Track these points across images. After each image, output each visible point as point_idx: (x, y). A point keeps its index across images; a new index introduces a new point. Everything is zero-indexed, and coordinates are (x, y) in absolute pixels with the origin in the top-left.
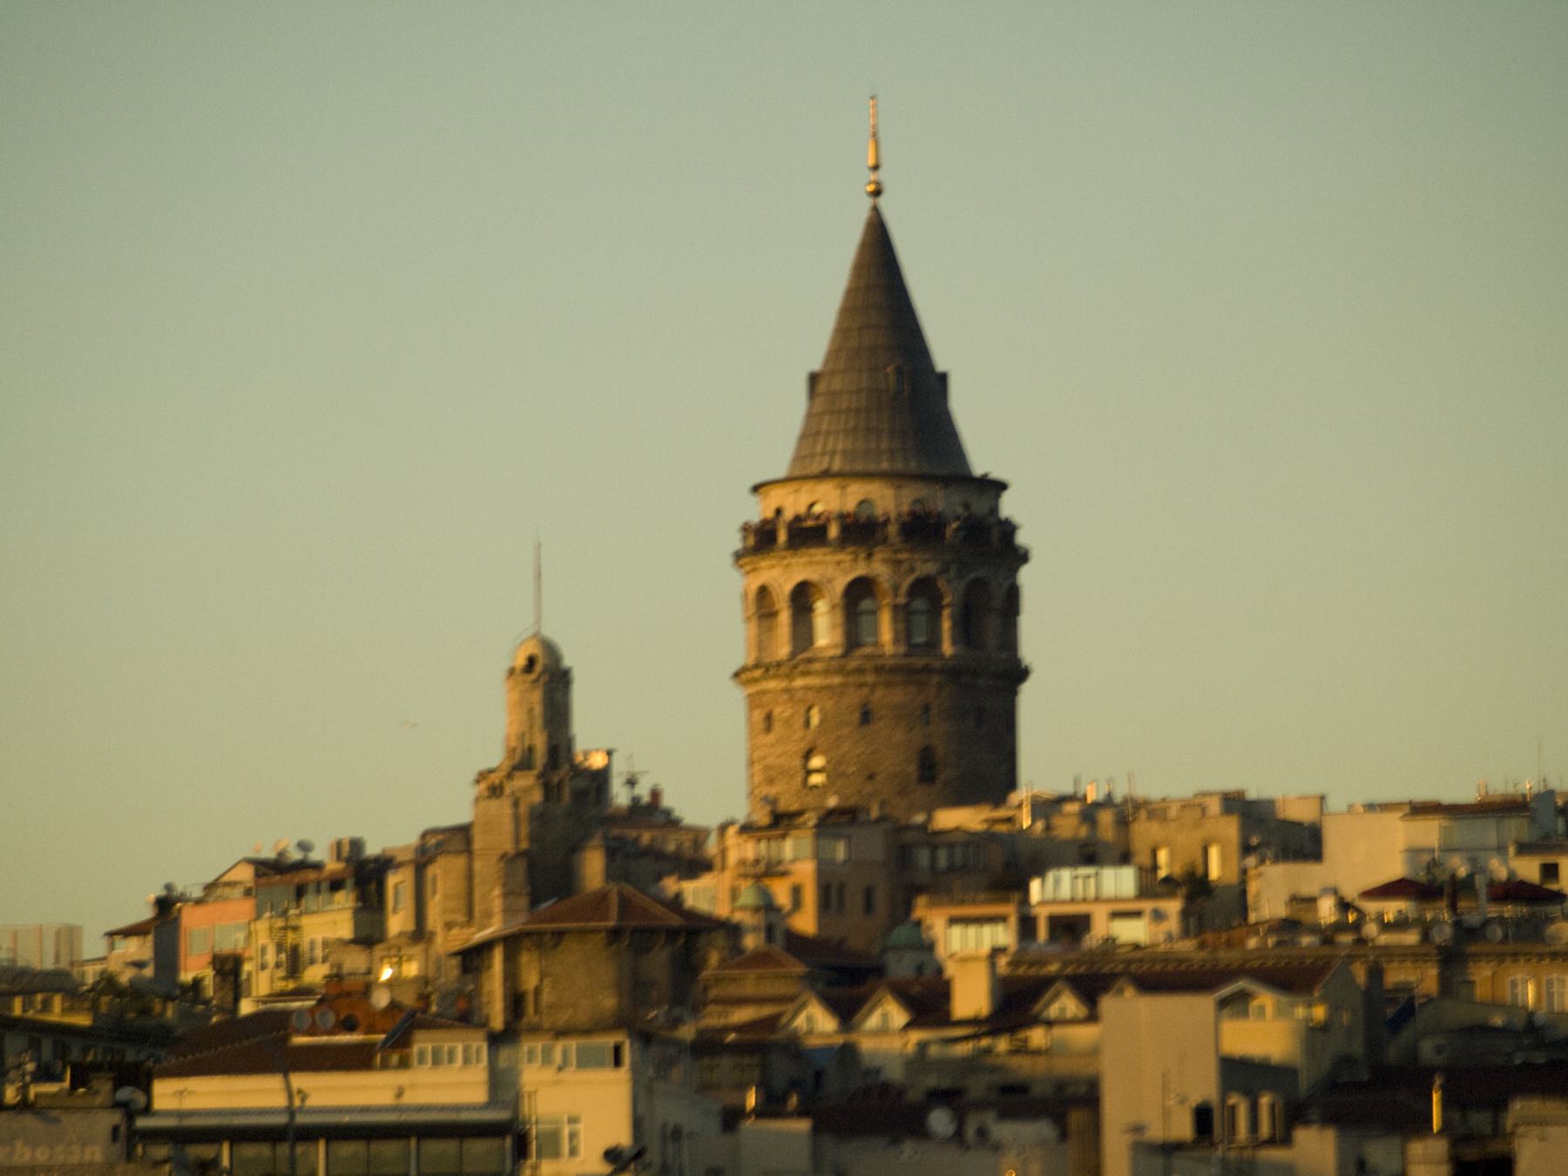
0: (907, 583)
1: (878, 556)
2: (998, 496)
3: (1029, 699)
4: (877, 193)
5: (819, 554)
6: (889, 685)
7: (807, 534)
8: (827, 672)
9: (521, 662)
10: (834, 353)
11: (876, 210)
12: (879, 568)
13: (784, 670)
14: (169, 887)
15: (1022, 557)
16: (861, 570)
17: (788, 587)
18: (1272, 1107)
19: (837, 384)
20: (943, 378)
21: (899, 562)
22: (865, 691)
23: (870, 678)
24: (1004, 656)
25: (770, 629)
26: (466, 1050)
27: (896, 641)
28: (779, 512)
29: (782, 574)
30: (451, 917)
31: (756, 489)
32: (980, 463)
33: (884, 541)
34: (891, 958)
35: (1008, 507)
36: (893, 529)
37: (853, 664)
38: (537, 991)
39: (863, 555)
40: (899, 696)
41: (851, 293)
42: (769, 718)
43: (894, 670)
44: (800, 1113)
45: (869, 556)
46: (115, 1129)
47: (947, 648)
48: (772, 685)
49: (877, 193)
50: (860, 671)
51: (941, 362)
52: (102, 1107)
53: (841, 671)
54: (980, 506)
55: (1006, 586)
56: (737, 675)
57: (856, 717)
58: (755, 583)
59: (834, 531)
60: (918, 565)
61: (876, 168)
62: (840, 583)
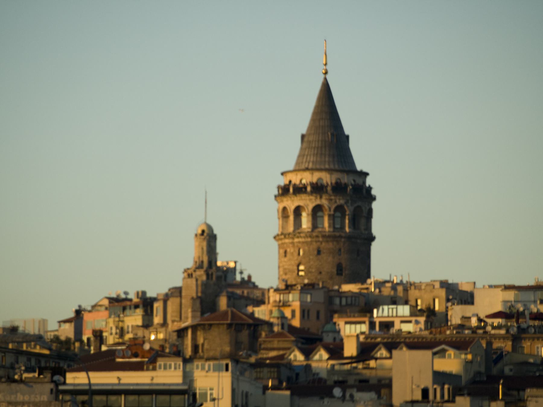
0: (334, 207)
1: (324, 197)
2: (366, 177)
3: (374, 247)
4: (326, 73)
5: (304, 196)
6: (327, 241)
7: (299, 190)
8: (306, 237)
9: (200, 232)
10: (310, 128)
11: (326, 79)
12: (324, 202)
13: (291, 236)
14: (80, 306)
15: (374, 198)
16: (318, 202)
17: (293, 208)
18: (449, 389)
19: (311, 138)
20: (347, 137)
21: (331, 200)
22: (319, 244)
23: (321, 239)
24: (366, 232)
25: (287, 222)
26: (175, 364)
27: (329, 226)
28: (290, 182)
29: (291, 203)
30: (174, 319)
31: (282, 174)
32: (360, 166)
33: (327, 192)
34: (324, 335)
35: (369, 181)
36: (329, 189)
37: (314, 234)
38: (203, 345)
39: (318, 197)
40: (331, 245)
41: (317, 107)
42: (286, 252)
43: (329, 237)
44: (287, 389)
45: (321, 197)
46: (52, 390)
47: (347, 229)
48: (287, 241)
49: (326, 73)
50: (317, 237)
51: (347, 132)
52: (47, 382)
53: (310, 237)
54: (359, 181)
55: (368, 208)
56: (275, 238)
57: (316, 252)
58: (281, 206)
59: (309, 189)
60: (338, 201)
61: (326, 64)
62: (311, 206)
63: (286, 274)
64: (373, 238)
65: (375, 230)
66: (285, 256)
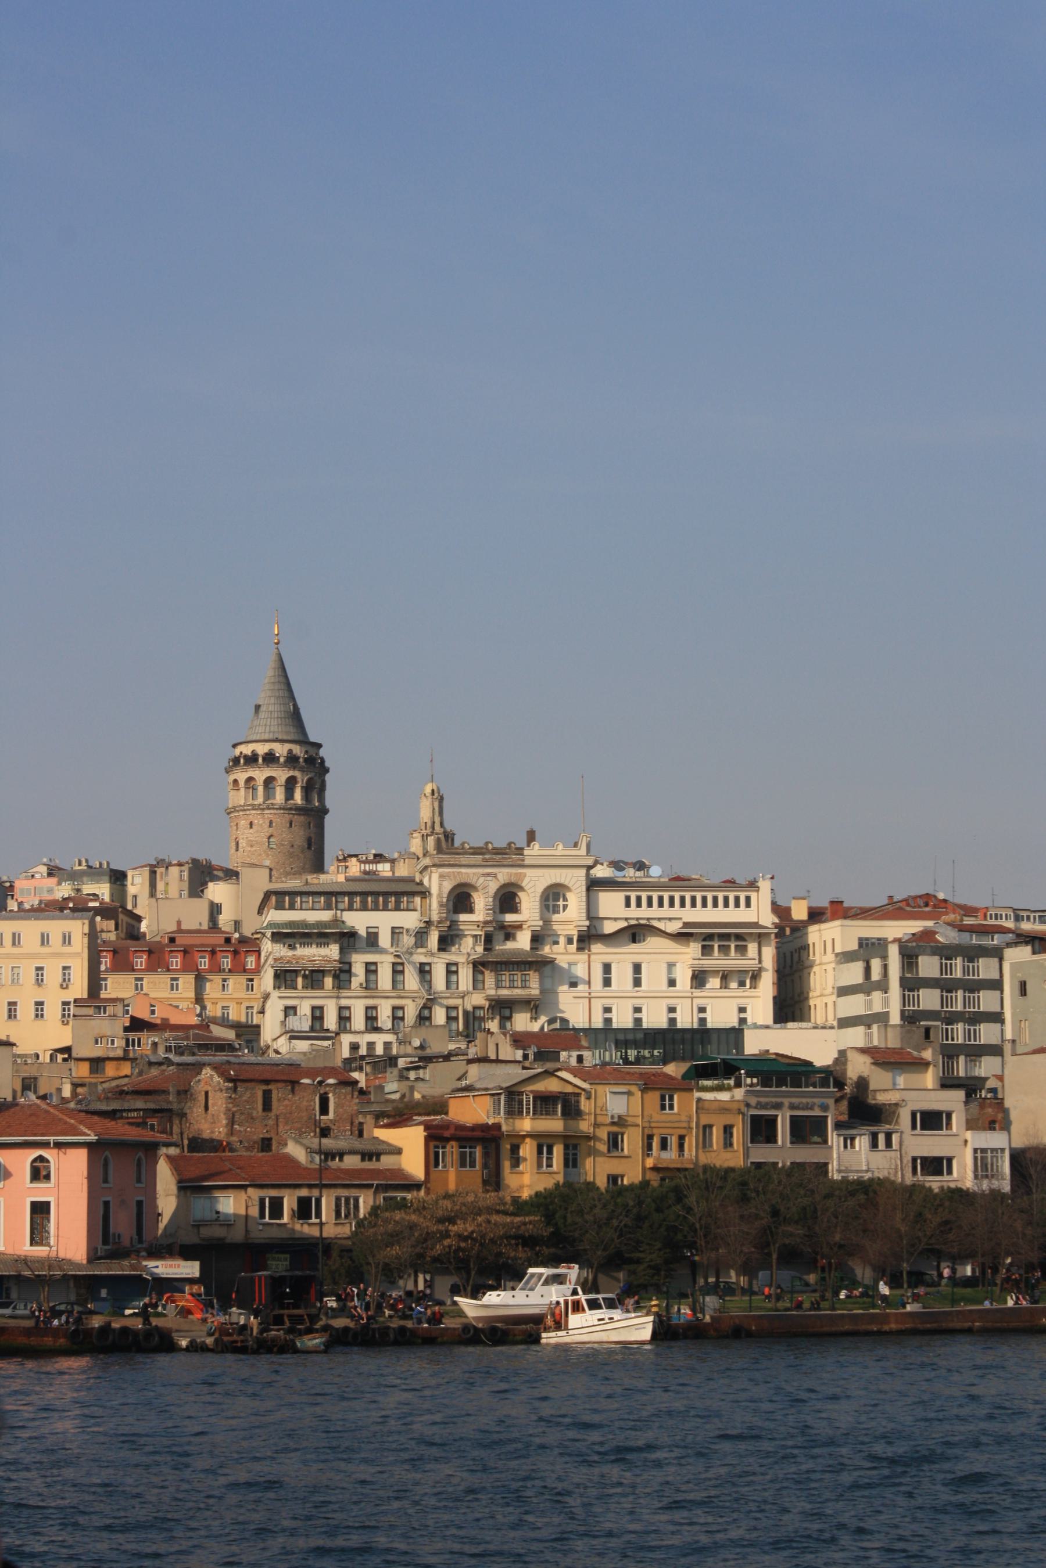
8: (280, 809)
12: (297, 774)
16: (291, 773)
17: (264, 778)
19: (271, 708)
26: (1006, 915)
27: (302, 799)
28: (241, 753)
32: (313, 738)
42: (251, 824)
47: (317, 804)
57: (288, 825)
58: (232, 778)
59: (282, 760)
63: (252, 846)
64: (326, 811)
65: (328, 804)
66: (251, 827)
